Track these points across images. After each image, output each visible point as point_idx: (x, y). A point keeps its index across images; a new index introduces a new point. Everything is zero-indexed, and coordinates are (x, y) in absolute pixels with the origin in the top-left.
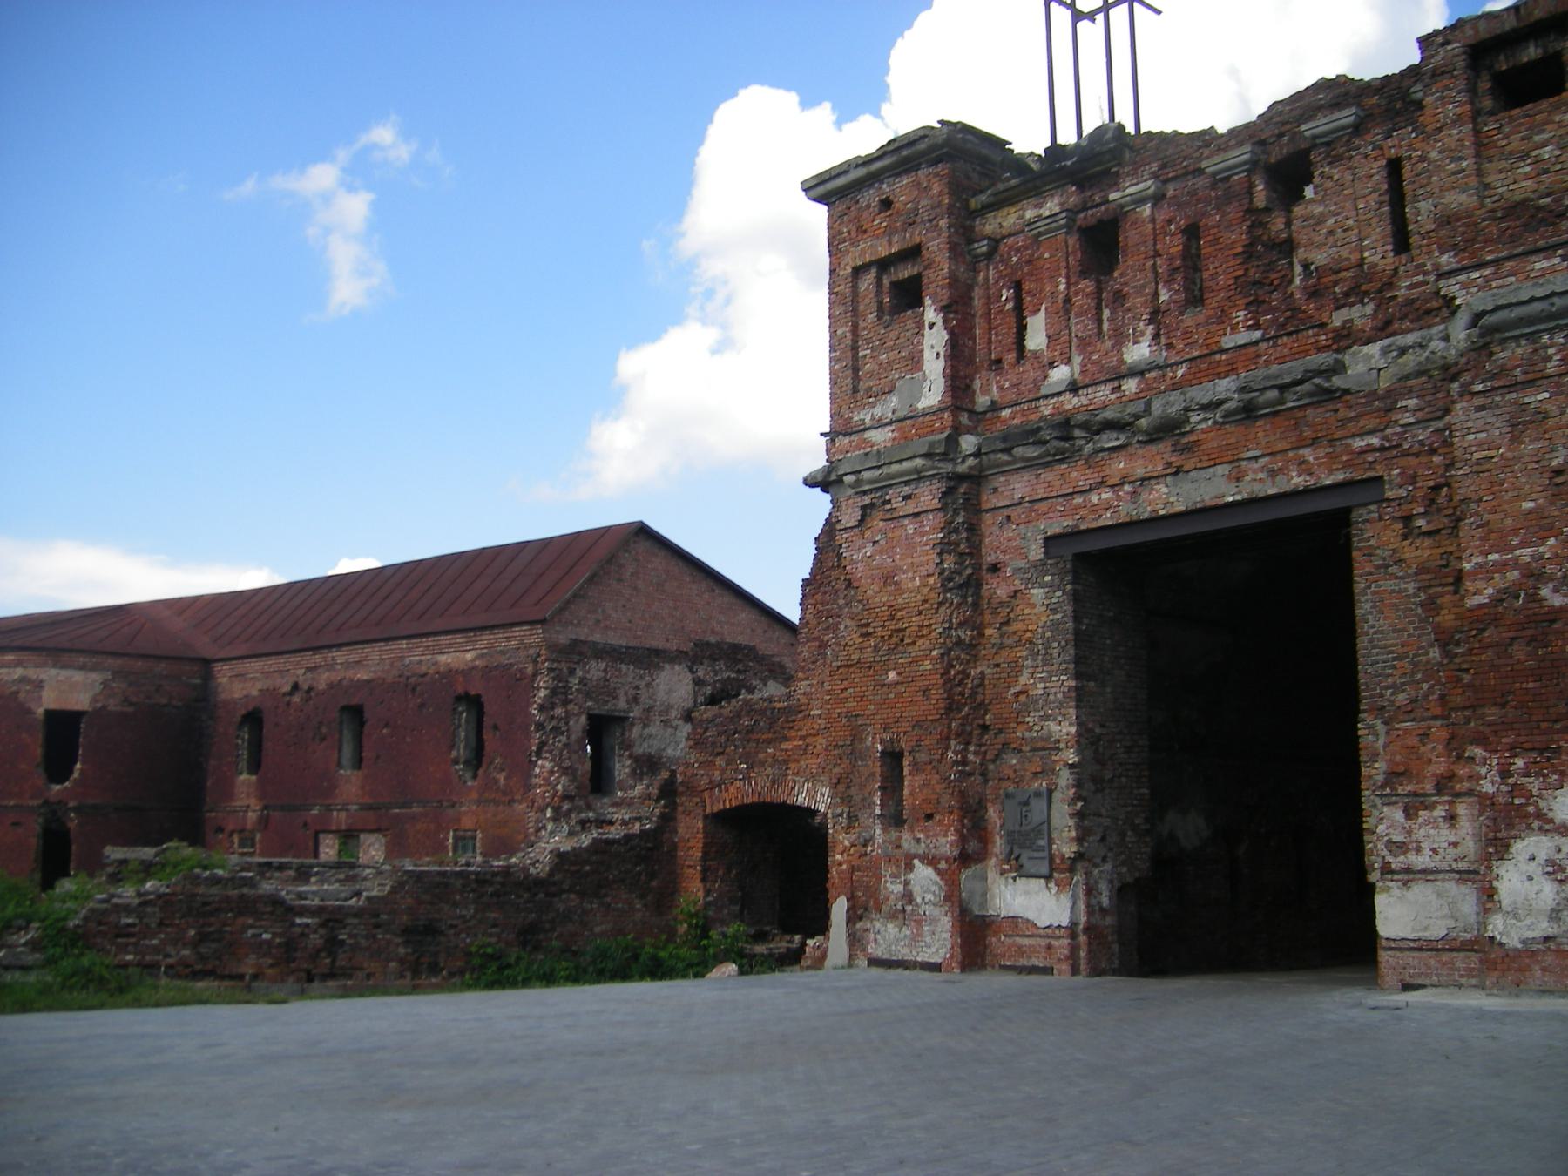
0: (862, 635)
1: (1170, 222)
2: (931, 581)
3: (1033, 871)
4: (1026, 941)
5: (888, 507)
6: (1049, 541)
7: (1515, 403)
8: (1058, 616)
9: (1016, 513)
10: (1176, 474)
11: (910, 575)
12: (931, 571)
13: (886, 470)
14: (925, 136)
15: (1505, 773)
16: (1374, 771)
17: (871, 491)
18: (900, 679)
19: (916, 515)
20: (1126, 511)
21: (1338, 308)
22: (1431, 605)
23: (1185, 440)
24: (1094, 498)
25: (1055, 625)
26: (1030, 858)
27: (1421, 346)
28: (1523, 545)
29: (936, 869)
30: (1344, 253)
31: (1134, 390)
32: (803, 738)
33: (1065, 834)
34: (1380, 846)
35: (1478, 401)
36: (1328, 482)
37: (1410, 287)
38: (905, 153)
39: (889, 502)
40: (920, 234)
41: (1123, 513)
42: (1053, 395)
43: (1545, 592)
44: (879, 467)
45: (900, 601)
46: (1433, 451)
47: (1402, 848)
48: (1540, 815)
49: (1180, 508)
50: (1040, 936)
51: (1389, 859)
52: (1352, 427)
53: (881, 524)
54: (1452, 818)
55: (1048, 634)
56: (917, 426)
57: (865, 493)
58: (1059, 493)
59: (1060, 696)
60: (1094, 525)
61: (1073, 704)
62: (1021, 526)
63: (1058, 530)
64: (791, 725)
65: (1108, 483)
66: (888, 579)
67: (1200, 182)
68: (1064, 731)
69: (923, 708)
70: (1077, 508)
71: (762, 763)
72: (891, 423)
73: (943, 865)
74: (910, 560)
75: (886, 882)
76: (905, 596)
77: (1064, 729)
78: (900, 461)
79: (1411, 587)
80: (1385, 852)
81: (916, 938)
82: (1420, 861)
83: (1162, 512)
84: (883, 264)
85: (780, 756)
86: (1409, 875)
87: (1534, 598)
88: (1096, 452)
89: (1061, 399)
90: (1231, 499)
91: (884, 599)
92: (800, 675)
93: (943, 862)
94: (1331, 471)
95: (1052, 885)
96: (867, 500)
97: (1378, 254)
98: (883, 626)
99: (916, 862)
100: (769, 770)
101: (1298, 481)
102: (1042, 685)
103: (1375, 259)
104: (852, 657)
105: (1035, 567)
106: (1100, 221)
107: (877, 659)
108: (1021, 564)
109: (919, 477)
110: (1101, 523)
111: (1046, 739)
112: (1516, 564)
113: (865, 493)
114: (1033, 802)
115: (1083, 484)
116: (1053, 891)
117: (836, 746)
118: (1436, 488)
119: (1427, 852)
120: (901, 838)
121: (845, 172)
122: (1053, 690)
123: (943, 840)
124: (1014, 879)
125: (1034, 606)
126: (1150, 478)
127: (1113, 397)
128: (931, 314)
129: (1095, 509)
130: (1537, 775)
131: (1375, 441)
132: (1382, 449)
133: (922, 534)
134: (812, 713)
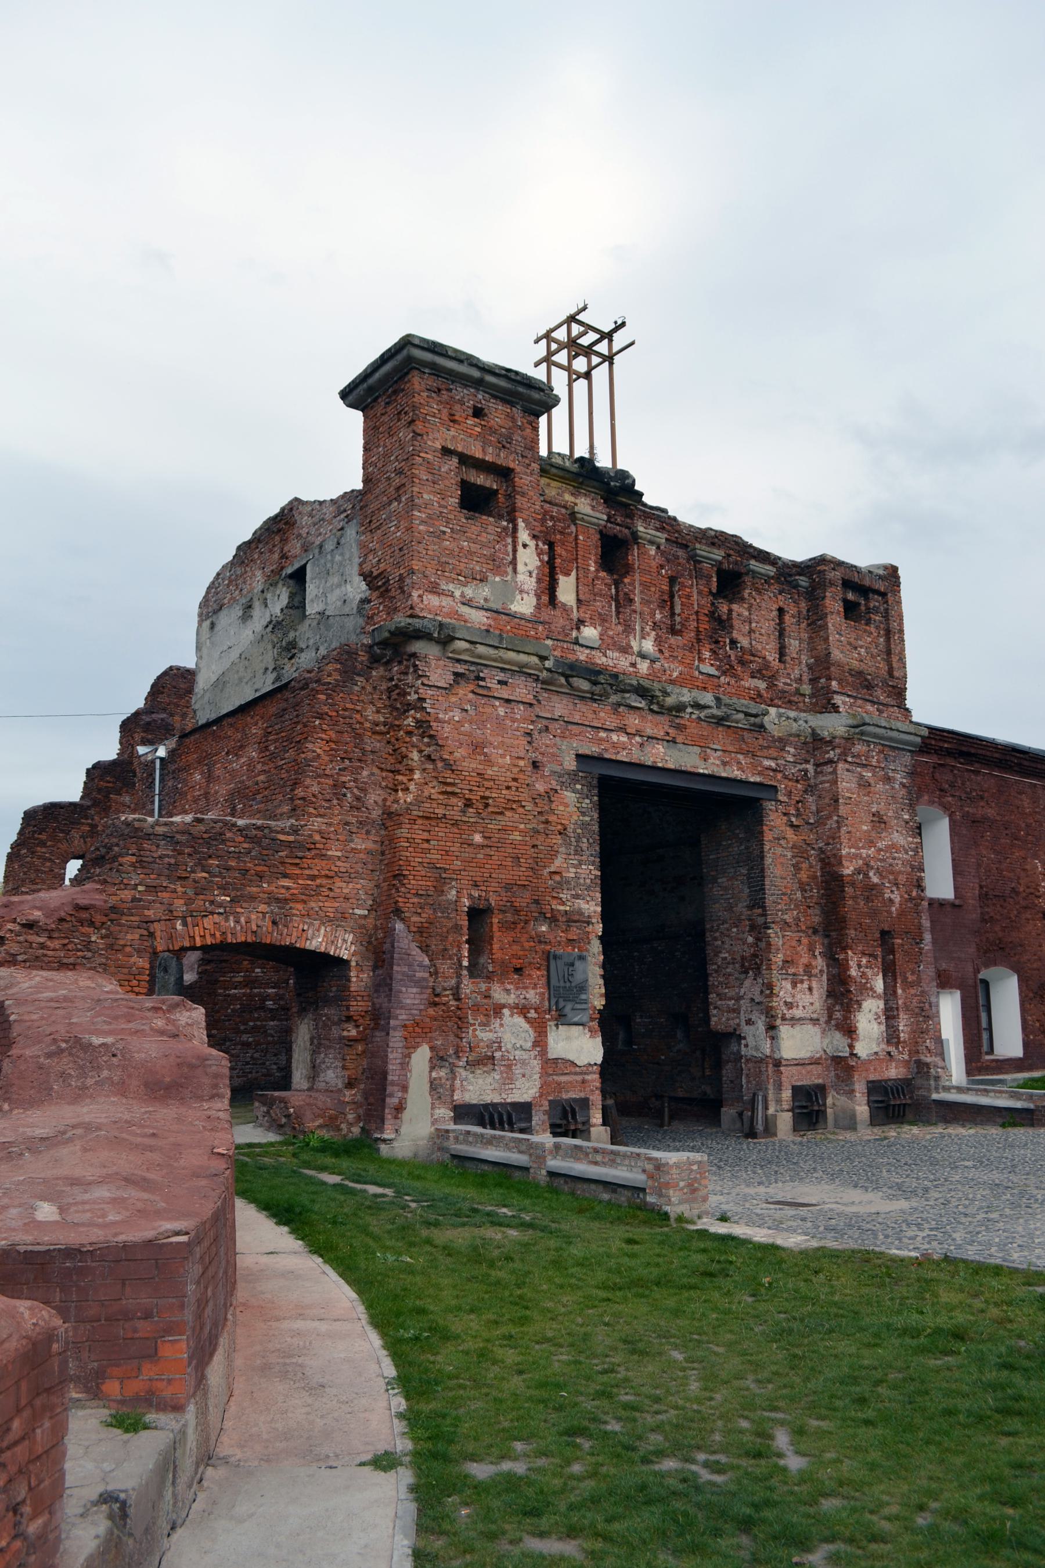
0: (442, 793)
1: (662, 567)
2: (522, 763)
3: (576, 1019)
4: (563, 1079)
5: (482, 683)
6: (579, 757)
7: (860, 774)
8: (587, 819)
9: (552, 726)
10: (668, 741)
11: (500, 752)
12: (522, 754)
13: (502, 653)
14: (543, 390)
15: (859, 966)
16: (778, 958)
17: (466, 662)
18: (486, 842)
19: (508, 701)
20: (636, 755)
21: (753, 677)
22: (797, 867)
23: (677, 721)
24: (614, 737)
25: (584, 825)
26: (573, 1009)
27: (795, 720)
28: (863, 848)
29: (525, 1017)
30: (760, 648)
31: (645, 672)
32: (313, 878)
33: (595, 991)
34: (782, 1004)
35: (847, 766)
36: (752, 780)
37: (785, 684)
38: (521, 389)
39: (483, 679)
40: (514, 461)
41: (635, 756)
42: (587, 647)
43: (871, 874)
44: (496, 648)
45: (489, 772)
46: (797, 781)
47: (789, 1005)
48: (872, 989)
49: (671, 766)
50: (576, 1074)
51: (785, 1012)
52: (765, 753)
53: (471, 696)
54: (810, 989)
55: (579, 831)
56: (512, 624)
57: (458, 661)
58: (592, 724)
59: (588, 881)
60: (613, 757)
61: (598, 889)
62: (557, 739)
63: (588, 752)
64: (297, 861)
65: (629, 731)
66: (477, 747)
67: (681, 553)
68: (592, 909)
69: (512, 873)
70: (601, 740)
71: (252, 898)
72: (482, 608)
73: (532, 1014)
74: (500, 739)
75: (475, 1030)
76: (495, 769)
77: (592, 907)
78: (519, 652)
79: (789, 854)
80: (783, 1008)
81: (509, 1079)
82: (798, 1013)
83: (660, 765)
84: (465, 460)
85: (283, 894)
86: (794, 1021)
87: (866, 876)
88: (619, 705)
89: (593, 653)
90: (701, 771)
91: (474, 766)
92: (312, 810)
93: (532, 1011)
94: (754, 774)
95: (587, 1031)
96: (460, 669)
97: (772, 657)
98: (470, 790)
99: (506, 1012)
100: (262, 907)
101: (737, 774)
102: (574, 870)
103: (771, 659)
104: (436, 811)
105: (569, 774)
106: (615, 536)
107: (464, 819)
108: (558, 769)
109: (521, 670)
110: (619, 758)
111: (580, 912)
112: (861, 858)
113: (458, 661)
114: (577, 963)
115: (608, 724)
116: (588, 1036)
117: (417, 895)
118: (798, 802)
119: (801, 1008)
120: (489, 989)
121: (461, 361)
122: (583, 876)
123: (532, 992)
124: (557, 1026)
125: (566, 805)
126: (652, 738)
127: (631, 669)
128: (524, 536)
129: (614, 745)
130: (871, 968)
131: (773, 764)
132: (774, 770)
133: (514, 721)
134: (329, 853)
